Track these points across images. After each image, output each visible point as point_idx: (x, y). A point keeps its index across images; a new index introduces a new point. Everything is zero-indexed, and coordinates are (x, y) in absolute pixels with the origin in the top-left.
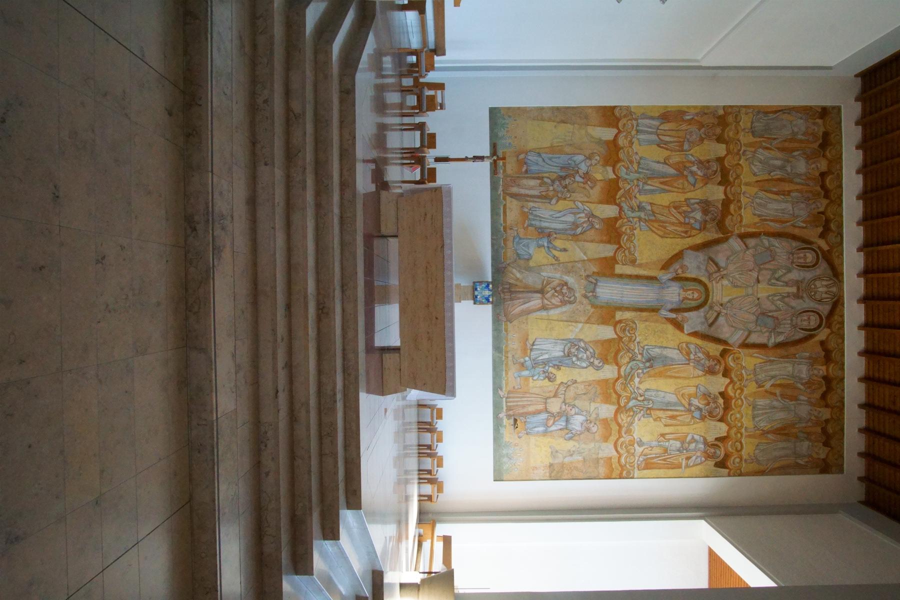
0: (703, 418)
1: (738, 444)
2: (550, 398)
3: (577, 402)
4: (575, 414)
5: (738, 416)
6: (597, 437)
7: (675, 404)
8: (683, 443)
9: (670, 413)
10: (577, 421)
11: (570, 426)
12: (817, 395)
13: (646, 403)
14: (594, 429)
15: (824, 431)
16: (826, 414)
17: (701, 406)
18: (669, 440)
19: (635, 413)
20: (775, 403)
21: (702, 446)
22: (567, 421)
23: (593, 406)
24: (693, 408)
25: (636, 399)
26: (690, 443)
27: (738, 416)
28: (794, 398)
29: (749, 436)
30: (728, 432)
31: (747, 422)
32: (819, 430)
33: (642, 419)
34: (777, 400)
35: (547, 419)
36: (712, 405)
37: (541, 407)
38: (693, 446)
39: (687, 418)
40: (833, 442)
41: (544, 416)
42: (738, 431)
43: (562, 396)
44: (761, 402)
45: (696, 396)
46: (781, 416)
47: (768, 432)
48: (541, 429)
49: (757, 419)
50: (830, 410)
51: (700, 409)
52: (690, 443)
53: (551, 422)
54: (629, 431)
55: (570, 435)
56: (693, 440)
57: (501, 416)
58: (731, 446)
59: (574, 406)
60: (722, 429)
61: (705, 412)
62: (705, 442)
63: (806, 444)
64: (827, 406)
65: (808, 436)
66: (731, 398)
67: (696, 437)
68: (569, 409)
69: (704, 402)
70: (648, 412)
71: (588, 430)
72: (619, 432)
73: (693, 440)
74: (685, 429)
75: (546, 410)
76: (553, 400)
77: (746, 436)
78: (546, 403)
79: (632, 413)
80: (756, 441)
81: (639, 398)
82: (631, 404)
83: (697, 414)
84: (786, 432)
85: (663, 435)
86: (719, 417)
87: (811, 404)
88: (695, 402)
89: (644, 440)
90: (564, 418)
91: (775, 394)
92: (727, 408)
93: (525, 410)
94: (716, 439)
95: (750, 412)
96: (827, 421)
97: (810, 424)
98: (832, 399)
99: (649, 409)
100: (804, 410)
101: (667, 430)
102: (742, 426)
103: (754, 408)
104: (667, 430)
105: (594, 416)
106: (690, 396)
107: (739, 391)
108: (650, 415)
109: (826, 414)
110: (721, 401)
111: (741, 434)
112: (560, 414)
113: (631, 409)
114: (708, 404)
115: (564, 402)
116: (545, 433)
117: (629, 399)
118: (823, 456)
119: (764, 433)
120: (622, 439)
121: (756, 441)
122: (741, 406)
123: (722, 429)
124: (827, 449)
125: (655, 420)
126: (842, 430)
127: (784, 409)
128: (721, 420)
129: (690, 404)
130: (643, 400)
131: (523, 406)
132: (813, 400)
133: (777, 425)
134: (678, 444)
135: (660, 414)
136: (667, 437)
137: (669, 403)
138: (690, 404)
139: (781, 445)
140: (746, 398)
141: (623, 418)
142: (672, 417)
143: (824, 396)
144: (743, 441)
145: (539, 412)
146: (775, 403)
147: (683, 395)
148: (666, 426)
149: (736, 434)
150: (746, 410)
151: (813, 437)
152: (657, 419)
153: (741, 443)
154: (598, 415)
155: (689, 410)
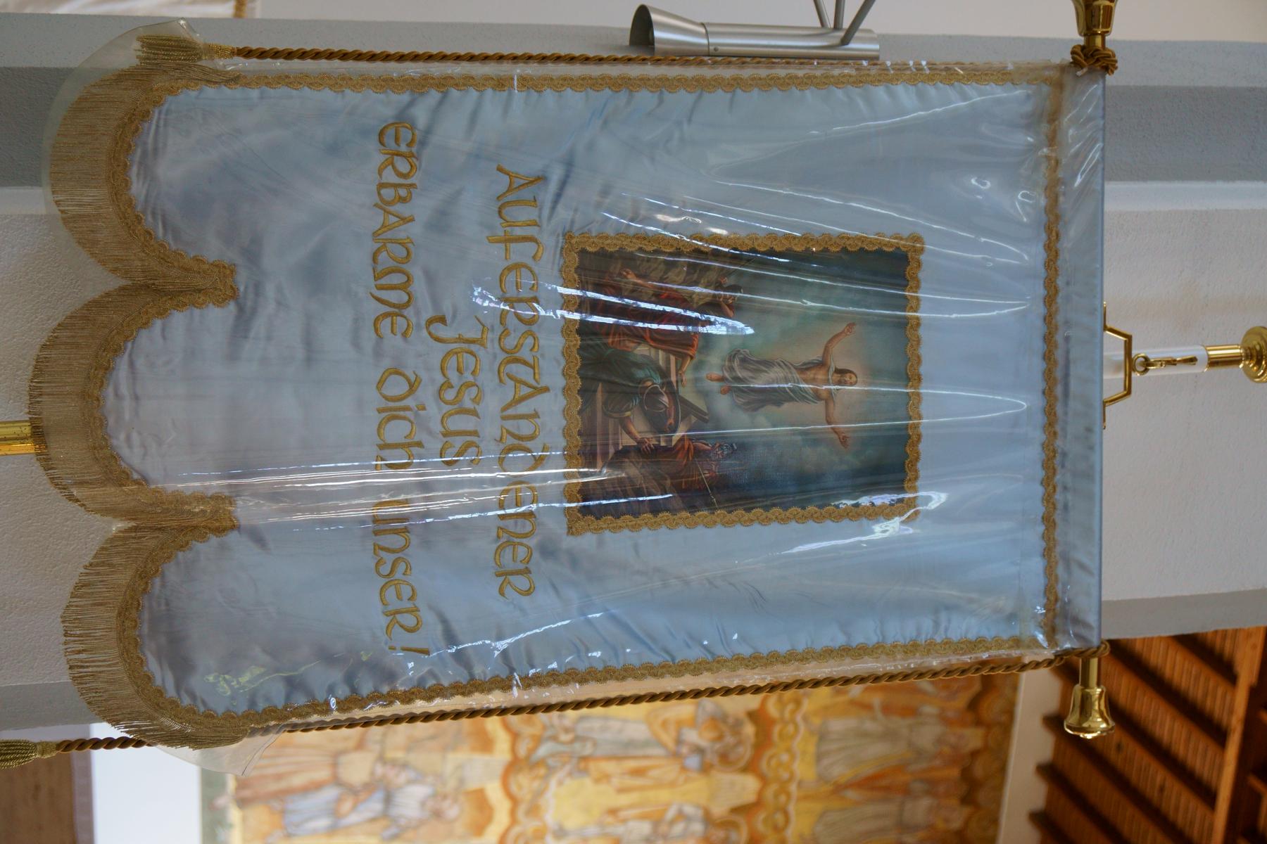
0: (705, 769)
1: (779, 818)
2: (344, 752)
3: (413, 758)
4: (410, 782)
5: (785, 757)
6: (459, 828)
7: (646, 744)
8: (657, 823)
9: (632, 764)
10: (411, 800)
11: (394, 812)
12: (962, 701)
13: (577, 746)
14: (452, 811)
15: (966, 774)
16: (973, 738)
17: (704, 743)
18: (624, 821)
19: (551, 770)
20: (869, 726)
21: (698, 827)
22: (388, 800)
23: (454, 758)
24: (684, 750)
25: (554, 738)
26: (672, 822)
27: (785, 757)
28: (911, 712)
29: (806, 798)
30: (760, 794)
31: (804, 769)
32: (954, 773)
33: (568, 782)
34: (874, 719)
35: (339, 800)
36: (730, 739)
37: (323, 774)
38: (679, 828)
39: (670, 771)
40: (982, 796)
41: (330, 793)
42: (783, 789)
43: (377, 747)
44: (837, 725)
45: (693, 723)
46: (876, 753)
47: (850, 785)
48: (323, 823)
49: (826, 762)
50: (980, 732)
51: (699, 751)
52: (672, 822)
53: (347, 806)
54: (534, 810)
55: (393, 830)
56: (681, 815)
57: (221, 802)
58: (765, 821)
59: (405, 766)
60: (747, 785)
61: (711, 758)
62: (708, 819)
63: (925, 803)
64: (978, 723)
65: (932, 787)
66: (772, 722)
67: (689, 810)
68: (391, 773)
69: (712, 735)
70: (582, 765)
71: (437, 814)
72: (513, 813)
73: (681, 815)
74: (664, 795)
75: (336, 781)
76: (356, 757)
77: (800, 799)
78: (335, 765)
79: (542, 771)
80: (818, 807)
81: (565, 737)
82: (543, 751)
83: (693, 761)
84: (884, 783)
85: (613, 812)
86: (742, 763)
87: (943, 719)
88: (692, 736)
89: (570, 824)
90: (379, 795)
91: (867, 707)
92: (763, 741)
93: (283, 785)
94: (736, 810)
95: (811, 749)
96: (974, 754)
97: (937, 762)
98: (992, 708)
99: (585, 759)
100: (928, 735)
101: (624, 800)
102: (791, 778)
103: (822, 736)
104: (624, 800)
105: (452, 784)
106: (680, 724)
107: (790, 707)
108: (584, 772)
109: (973, 738)
110: (749, 730)
111: (789, 795)
112: (370, 787)
113: (542, 762)
114: (720, 738)
115: (382, 759)
116: (332, 831)
117: (538, 741)
118: (956, 824)
119: (839, 789)
120: (516, 830)
121: (818, 807)
122: (793, 737)
123: (747, 785)
124: (966, 811)
125: (597, 781)
126: (1003, 770)
127: (889, 735)
128: (746, 770)
129: (679, 741)
130: (572, 742)
131: (279, 777)
132: (950, 714)
133: (867, 770)
134: (645, 828)
135: (610, 767)
136: (623, 814)
137: (631, 744)
138: (679, 741)
139: (870, 809)
140: (805, 719)
141: (524, 783)
142: (638, 772)
143: (974, 705)
144: (792, 808)
145: (317, 786)
146: (869, 726)
147: (665, 724)
148: (621, 790)
149: (776, 796)
150: (803, 743)
151: (941, 789)
152: (604, 778)
153: (786, 814)
154: (461, 781)
155: (676, 756)
